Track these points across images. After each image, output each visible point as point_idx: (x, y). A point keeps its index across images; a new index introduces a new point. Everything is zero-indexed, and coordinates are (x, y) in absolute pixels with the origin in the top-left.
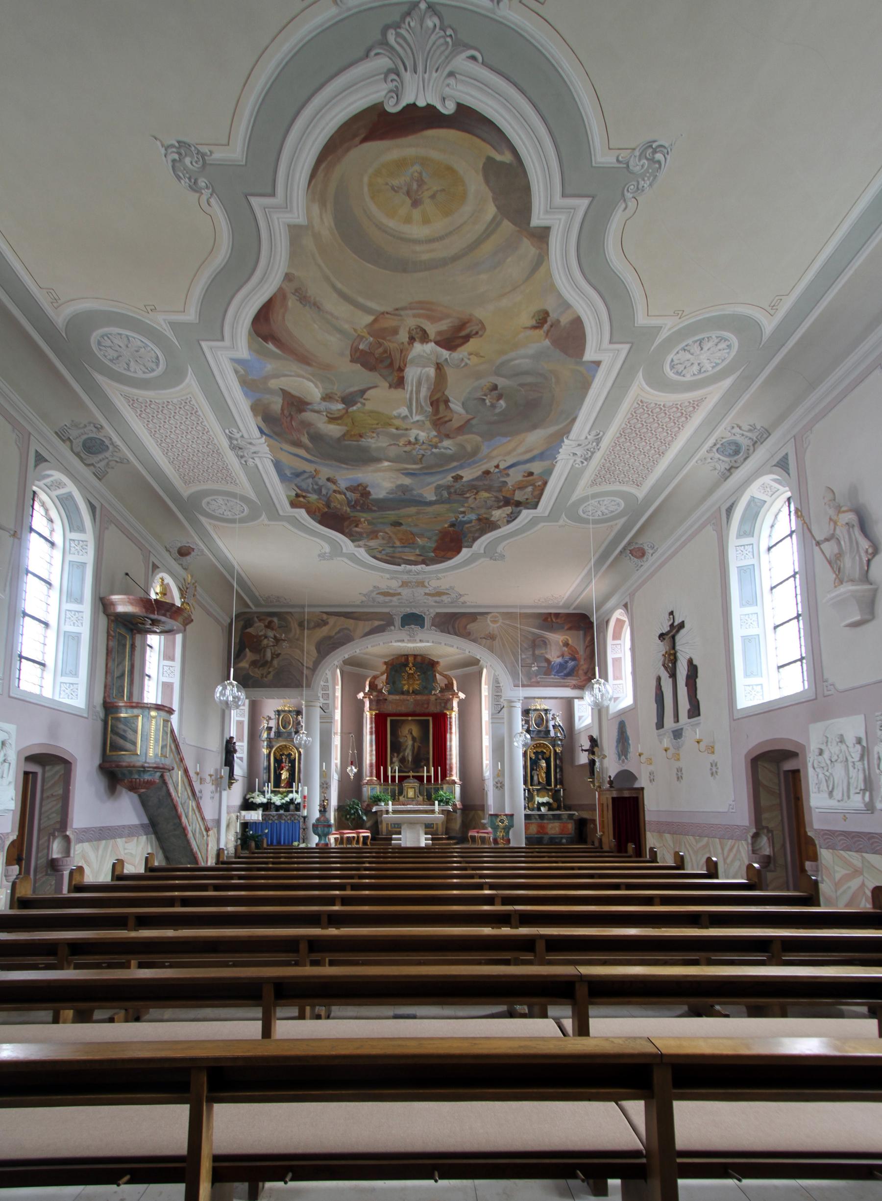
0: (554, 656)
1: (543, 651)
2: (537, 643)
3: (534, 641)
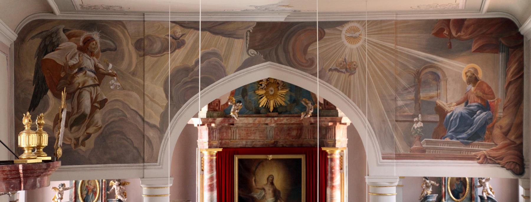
0: (452, 99)
1: (433, 93)
2: (425, 77)
3: (418, 74)
